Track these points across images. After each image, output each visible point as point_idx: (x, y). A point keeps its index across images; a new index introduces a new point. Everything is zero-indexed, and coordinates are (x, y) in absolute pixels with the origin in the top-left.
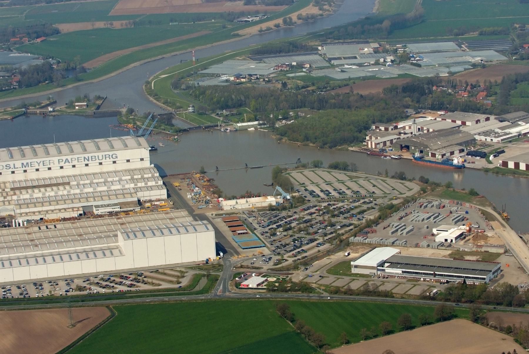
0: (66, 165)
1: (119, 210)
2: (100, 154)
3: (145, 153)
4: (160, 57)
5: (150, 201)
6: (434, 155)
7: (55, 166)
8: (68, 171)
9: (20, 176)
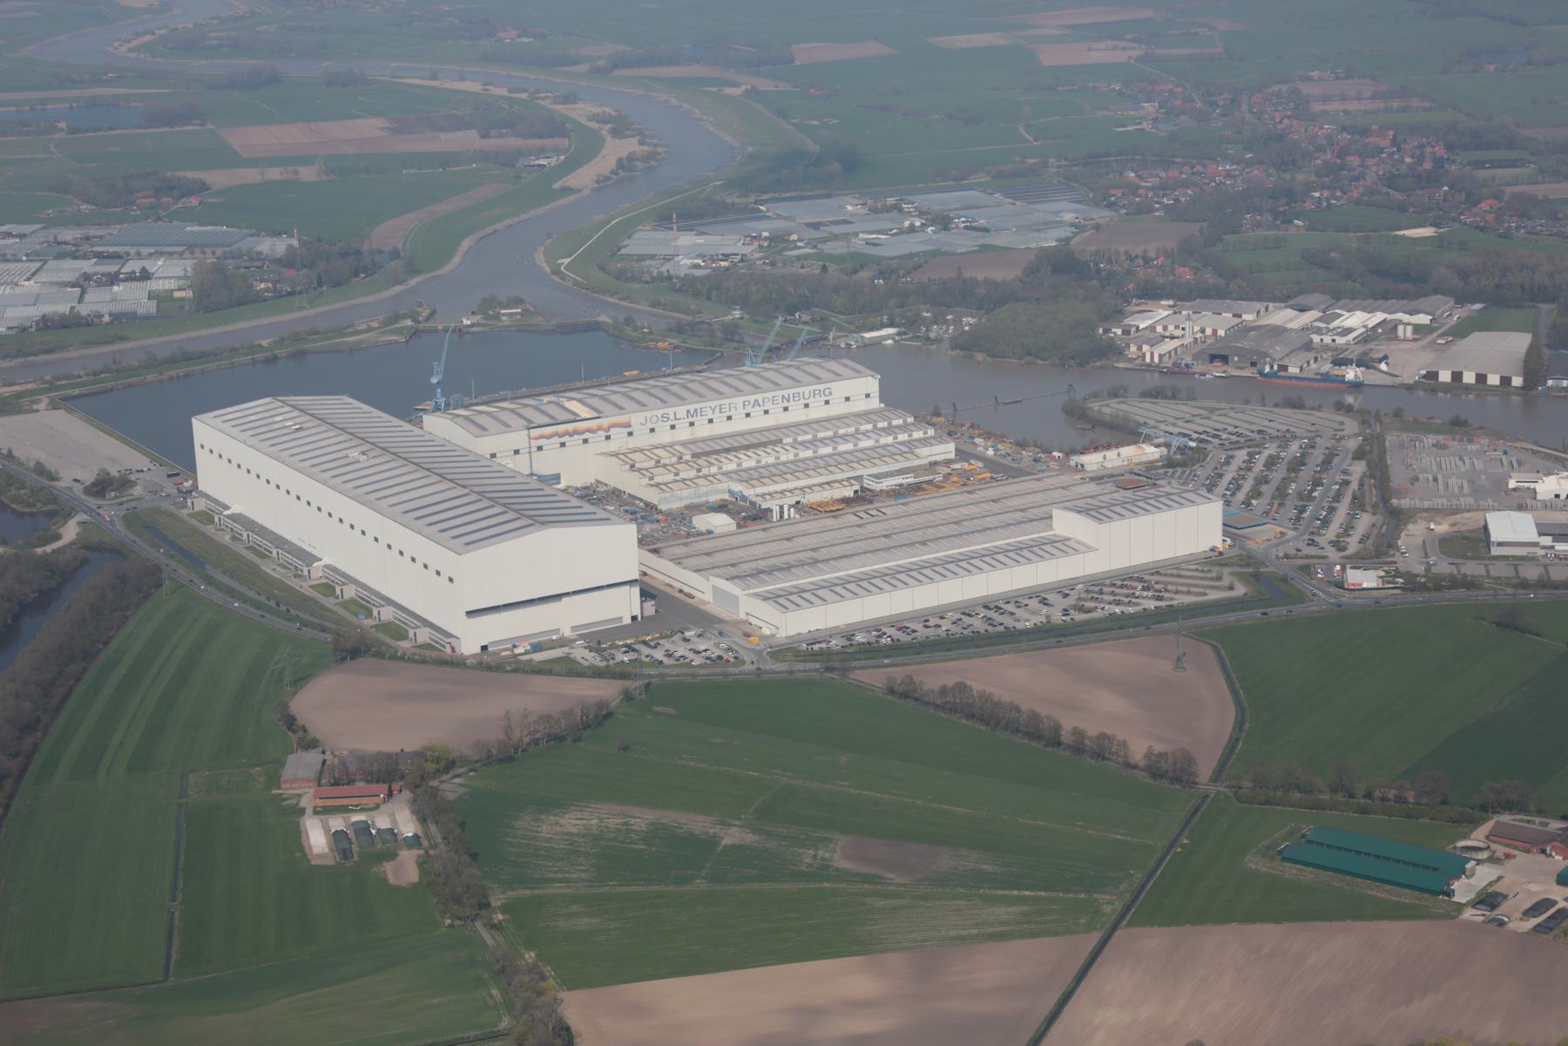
0: (757, 412)
1: (911, 480)
2: (806, 389)
3: (871, 384)
4: (489, 230)
5: (936, 463)
6: (1284, 368)
7: (738, 414)
8: (759, 421)
9: (683, 434)
